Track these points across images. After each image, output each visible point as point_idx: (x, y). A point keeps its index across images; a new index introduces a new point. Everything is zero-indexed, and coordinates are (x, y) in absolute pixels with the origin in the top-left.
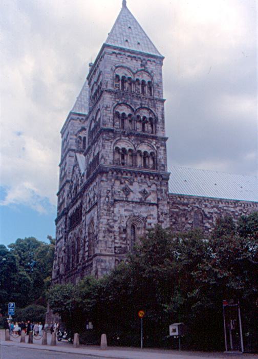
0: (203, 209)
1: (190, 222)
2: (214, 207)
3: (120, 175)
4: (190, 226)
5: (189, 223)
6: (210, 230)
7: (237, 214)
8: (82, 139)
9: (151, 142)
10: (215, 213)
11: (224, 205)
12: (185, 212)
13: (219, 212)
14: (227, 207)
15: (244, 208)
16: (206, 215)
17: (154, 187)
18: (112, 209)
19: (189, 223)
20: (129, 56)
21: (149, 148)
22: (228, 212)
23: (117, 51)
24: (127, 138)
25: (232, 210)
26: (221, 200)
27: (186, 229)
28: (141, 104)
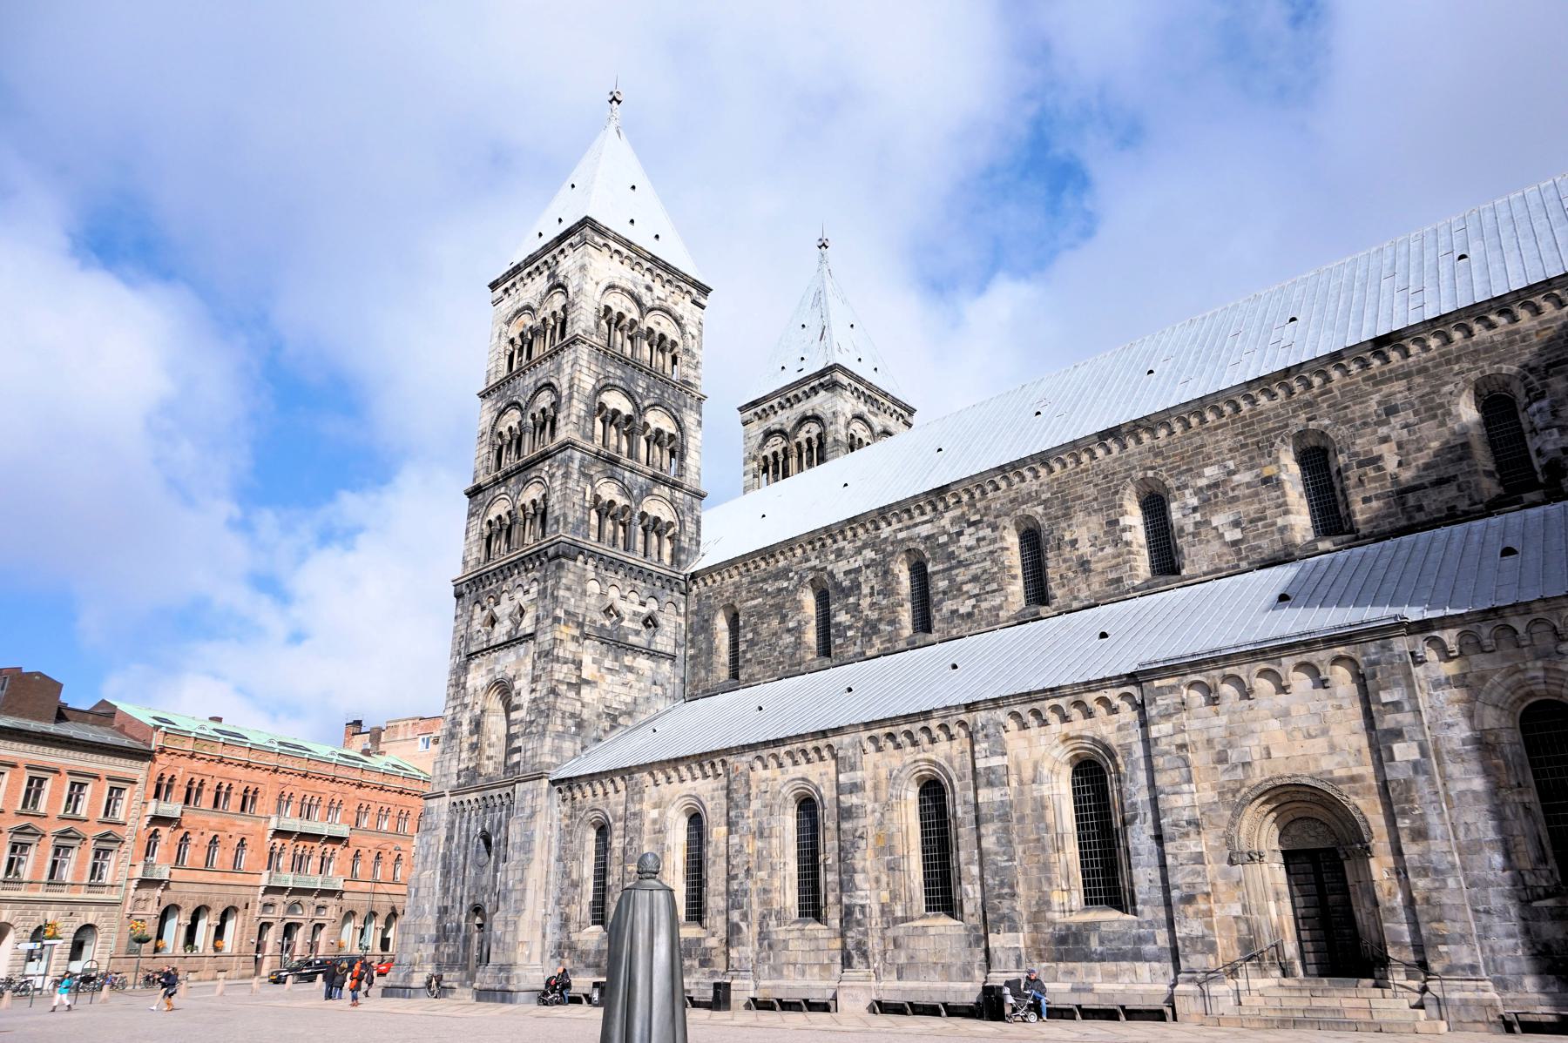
0: (829, 568)
1: (791, 625)
2: (865, 546)
3: (481, 590)
4: (793, 639)
5: (789, 631)
6: (850, 633)
7: (943, 539)
8: (771, 459)
9: (541, 470)
10: (867, 567)
11: (900, 526)
12: (779, 599)
13: (879, 557)
14: (908, 528)
15: (972, 505)
16: (838, 586)
17: (534, 589)
18: (462, 680)
19: (789, 631)
20: (529, 274)
21: (539, 486)
22: (912, 545)
23: (508, 284)
24: (503, 490)
25: (924, 534)
26: (883, 513)
27: (781, 653)
28: (536, 383)
